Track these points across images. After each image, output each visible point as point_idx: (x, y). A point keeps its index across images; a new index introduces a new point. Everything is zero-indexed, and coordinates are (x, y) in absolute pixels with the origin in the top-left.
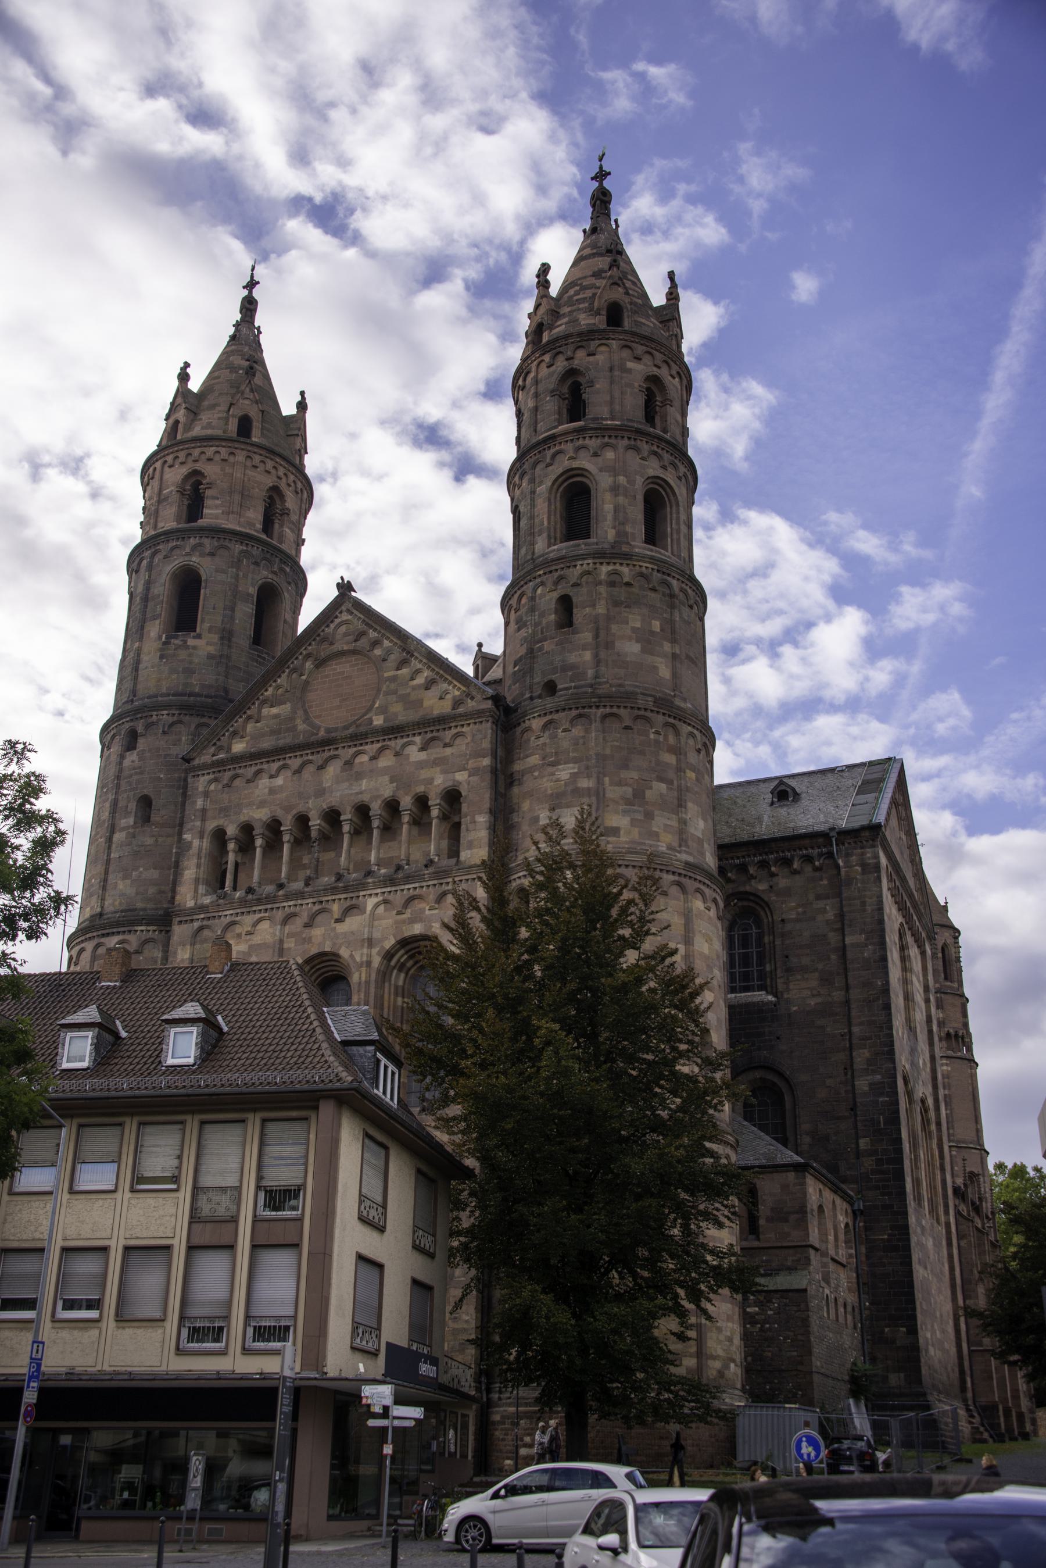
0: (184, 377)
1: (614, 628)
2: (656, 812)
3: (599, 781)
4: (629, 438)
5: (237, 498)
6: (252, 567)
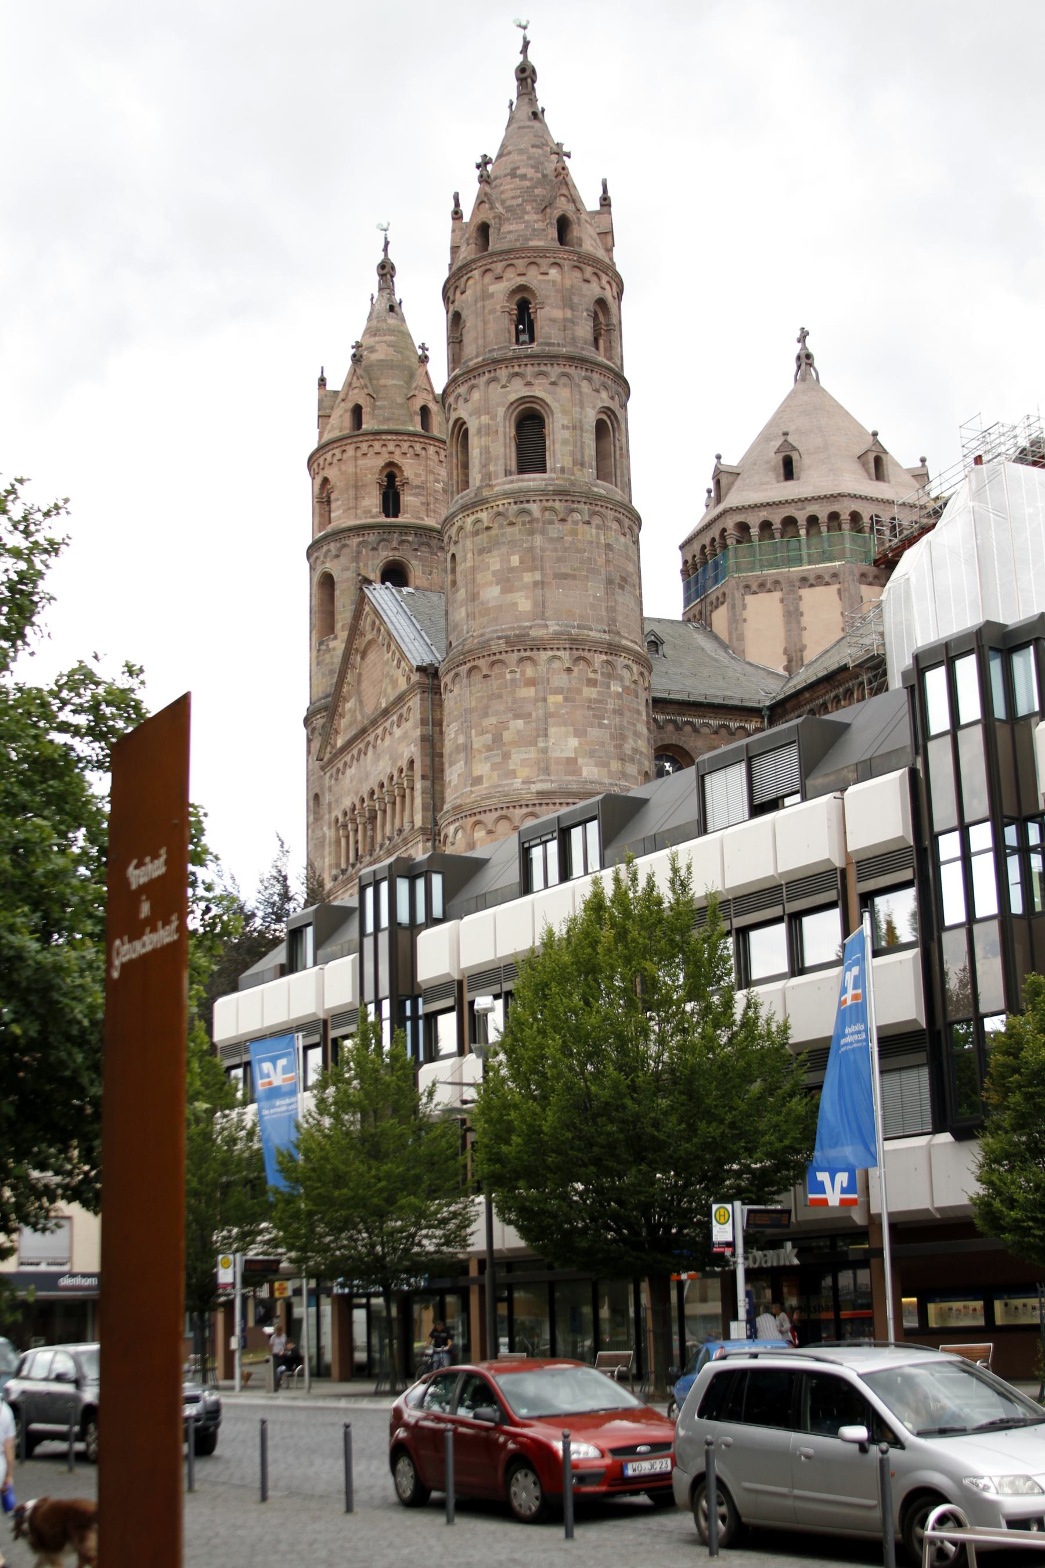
0: (322, 382)
1: (479, 577)
2: (513, 751)
3: (468, 737)
4: (490, 371)
5: (352, 492)
6: (371, 553)
